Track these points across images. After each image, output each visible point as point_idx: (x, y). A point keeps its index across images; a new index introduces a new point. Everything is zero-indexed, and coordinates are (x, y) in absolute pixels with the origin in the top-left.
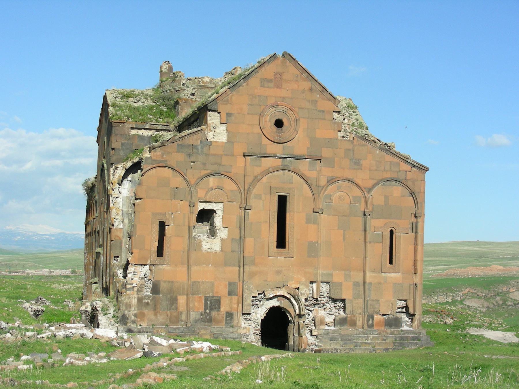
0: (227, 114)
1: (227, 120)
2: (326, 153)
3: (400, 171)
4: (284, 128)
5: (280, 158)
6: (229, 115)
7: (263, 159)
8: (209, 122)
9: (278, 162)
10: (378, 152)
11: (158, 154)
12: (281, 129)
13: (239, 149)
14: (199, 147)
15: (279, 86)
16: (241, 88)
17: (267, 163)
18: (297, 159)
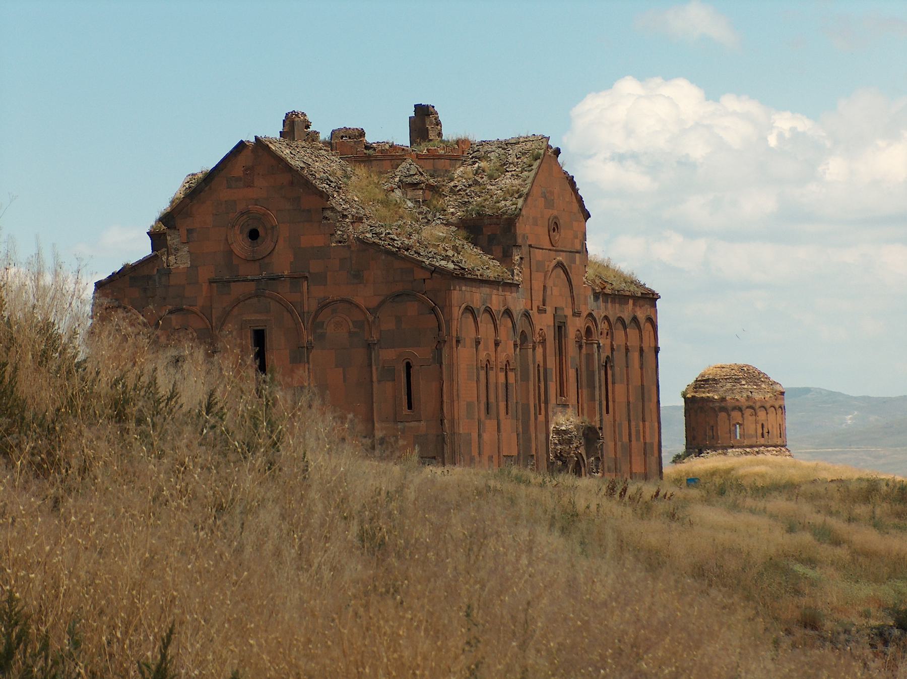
0: (187, 230)
1: (188, 238)
2: (315, 266)
3: (415, 280)
4: (259, 240)
5: (253, 280)
6: (190, 231)
7: (232, 284)
8: (169, 243)
9: (252, 287)
10: (383, 257)
11: (107, 292)
12: (255, 241)
13: (205, 273)
14: (157, 278)
15: (249, 185)
16: (202, 194)
17: (238, 289)
18: (274, 279)
